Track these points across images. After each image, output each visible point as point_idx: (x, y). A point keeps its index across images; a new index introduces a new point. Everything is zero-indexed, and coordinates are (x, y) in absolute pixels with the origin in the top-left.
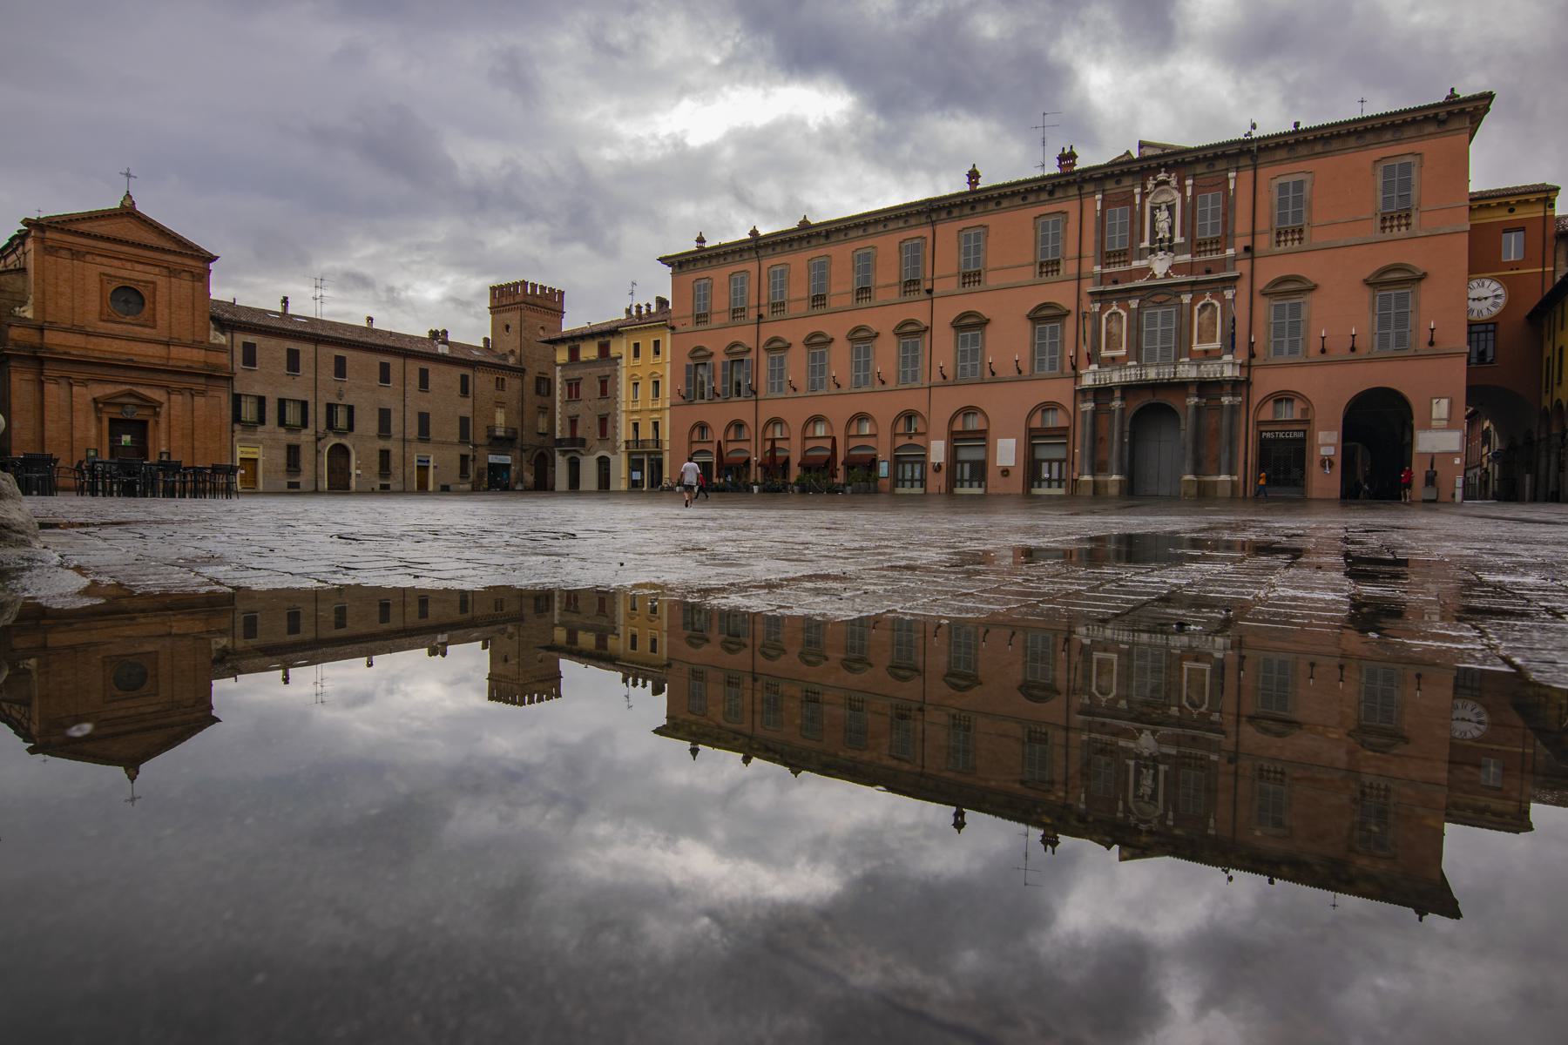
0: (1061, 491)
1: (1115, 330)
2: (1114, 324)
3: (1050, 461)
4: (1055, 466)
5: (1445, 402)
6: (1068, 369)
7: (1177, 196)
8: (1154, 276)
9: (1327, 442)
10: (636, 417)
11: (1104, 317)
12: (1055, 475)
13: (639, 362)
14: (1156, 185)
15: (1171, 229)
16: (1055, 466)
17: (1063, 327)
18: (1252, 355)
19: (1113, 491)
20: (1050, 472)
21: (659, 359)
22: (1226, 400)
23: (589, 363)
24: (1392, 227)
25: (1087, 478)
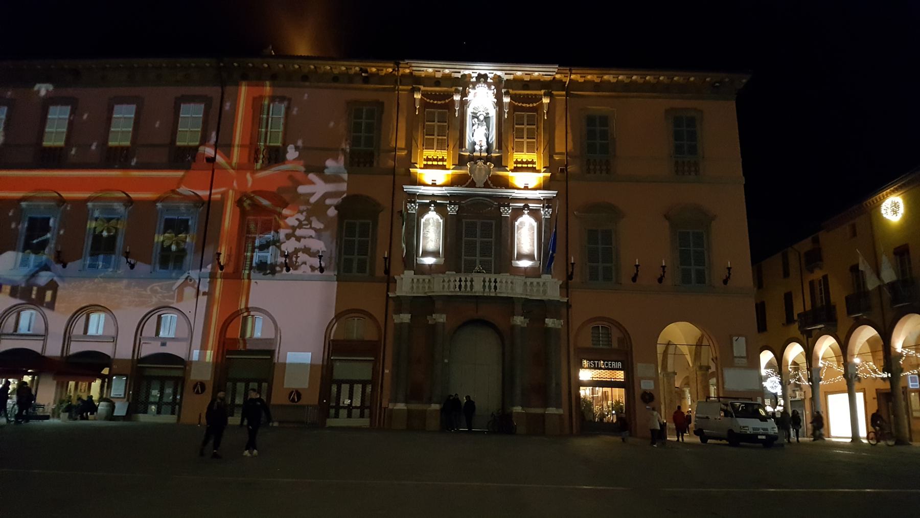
0: (365, 422)
3: (352, 383)
4: (358, 388)
5: (742, 340)
6: (380, 272)
12: (357, 402)
16: (358, 388)
17: (375, 224)
18: (570, 277)
19: (434, 423)
20: (351, 398)
22: (550, 322)
25: (401, 406)
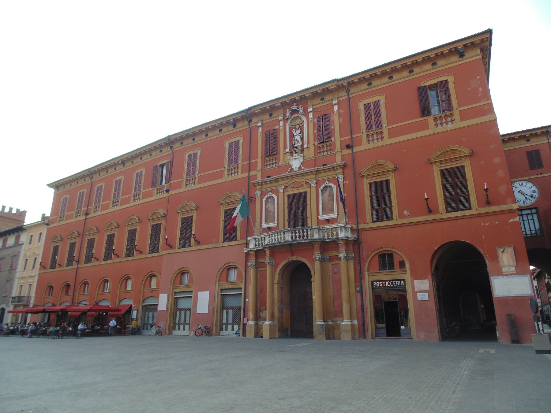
1: (271, 209)
2: (269, 205)
7: (304, 119)
8: (292, 169)
9: (421, 290)
10: (22, 281)
11: (264, 200)
13: (30, 246)
14: (292, 114)
15: (302, 139)
21: (40, 244)
23: (10, 247)
24: (442, 124)
